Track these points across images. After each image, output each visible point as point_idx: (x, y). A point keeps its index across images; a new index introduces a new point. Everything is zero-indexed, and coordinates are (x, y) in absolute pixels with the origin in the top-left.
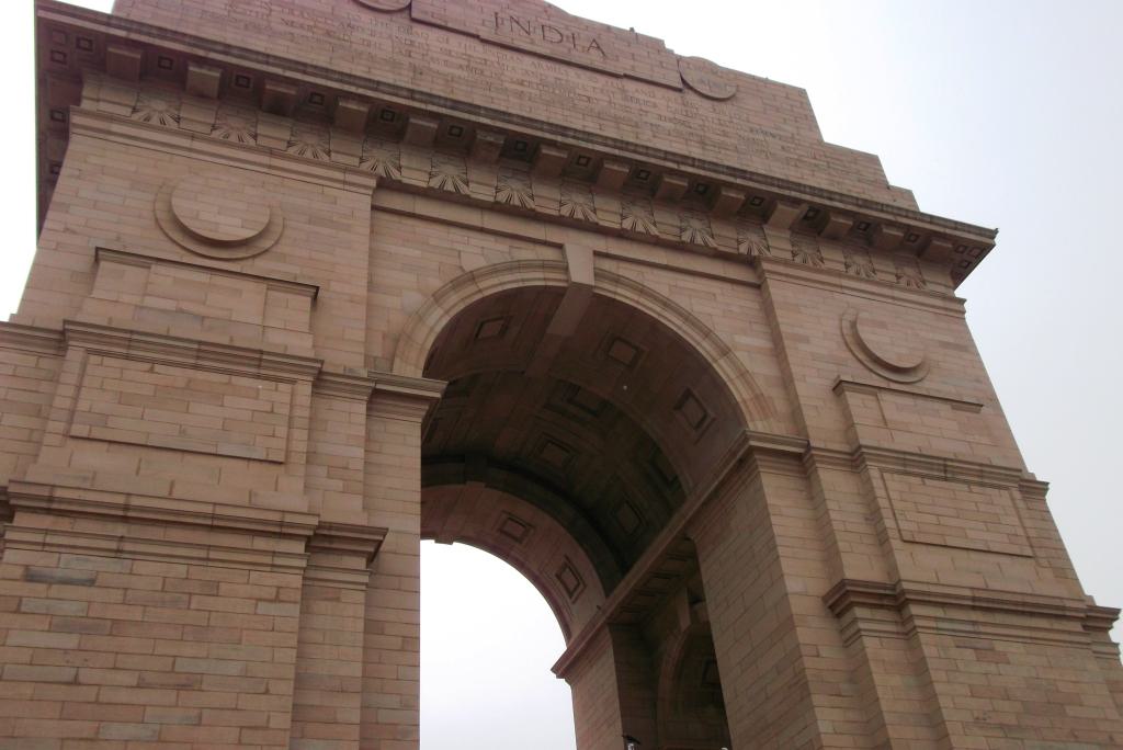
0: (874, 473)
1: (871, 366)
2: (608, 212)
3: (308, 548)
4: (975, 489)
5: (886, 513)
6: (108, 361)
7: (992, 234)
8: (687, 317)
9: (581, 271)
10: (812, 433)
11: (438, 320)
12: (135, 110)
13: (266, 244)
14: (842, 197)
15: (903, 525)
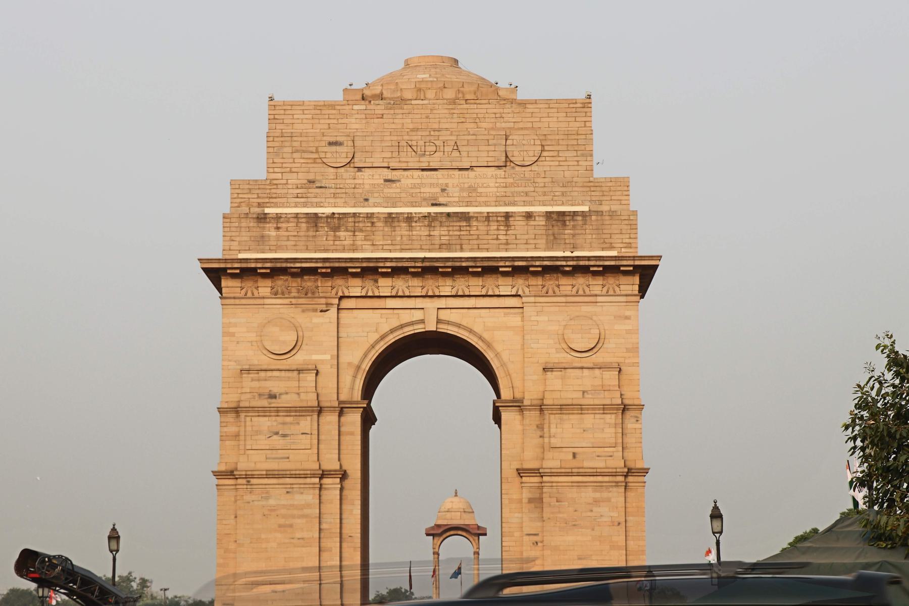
0: (547, 417)
1: (568, 350)
2: (446, 286)
3: (321, 478)
4: (598, 416)
5: (546, 435)
6: (254, 419)
7: (659, 258)
8: (480, 338)
9: (431, 327)
10: (526, 394)
11: (367, 365)
12: (242, 288)
13: (297, 348)
14: (565, 258)
15: (553, 440)
